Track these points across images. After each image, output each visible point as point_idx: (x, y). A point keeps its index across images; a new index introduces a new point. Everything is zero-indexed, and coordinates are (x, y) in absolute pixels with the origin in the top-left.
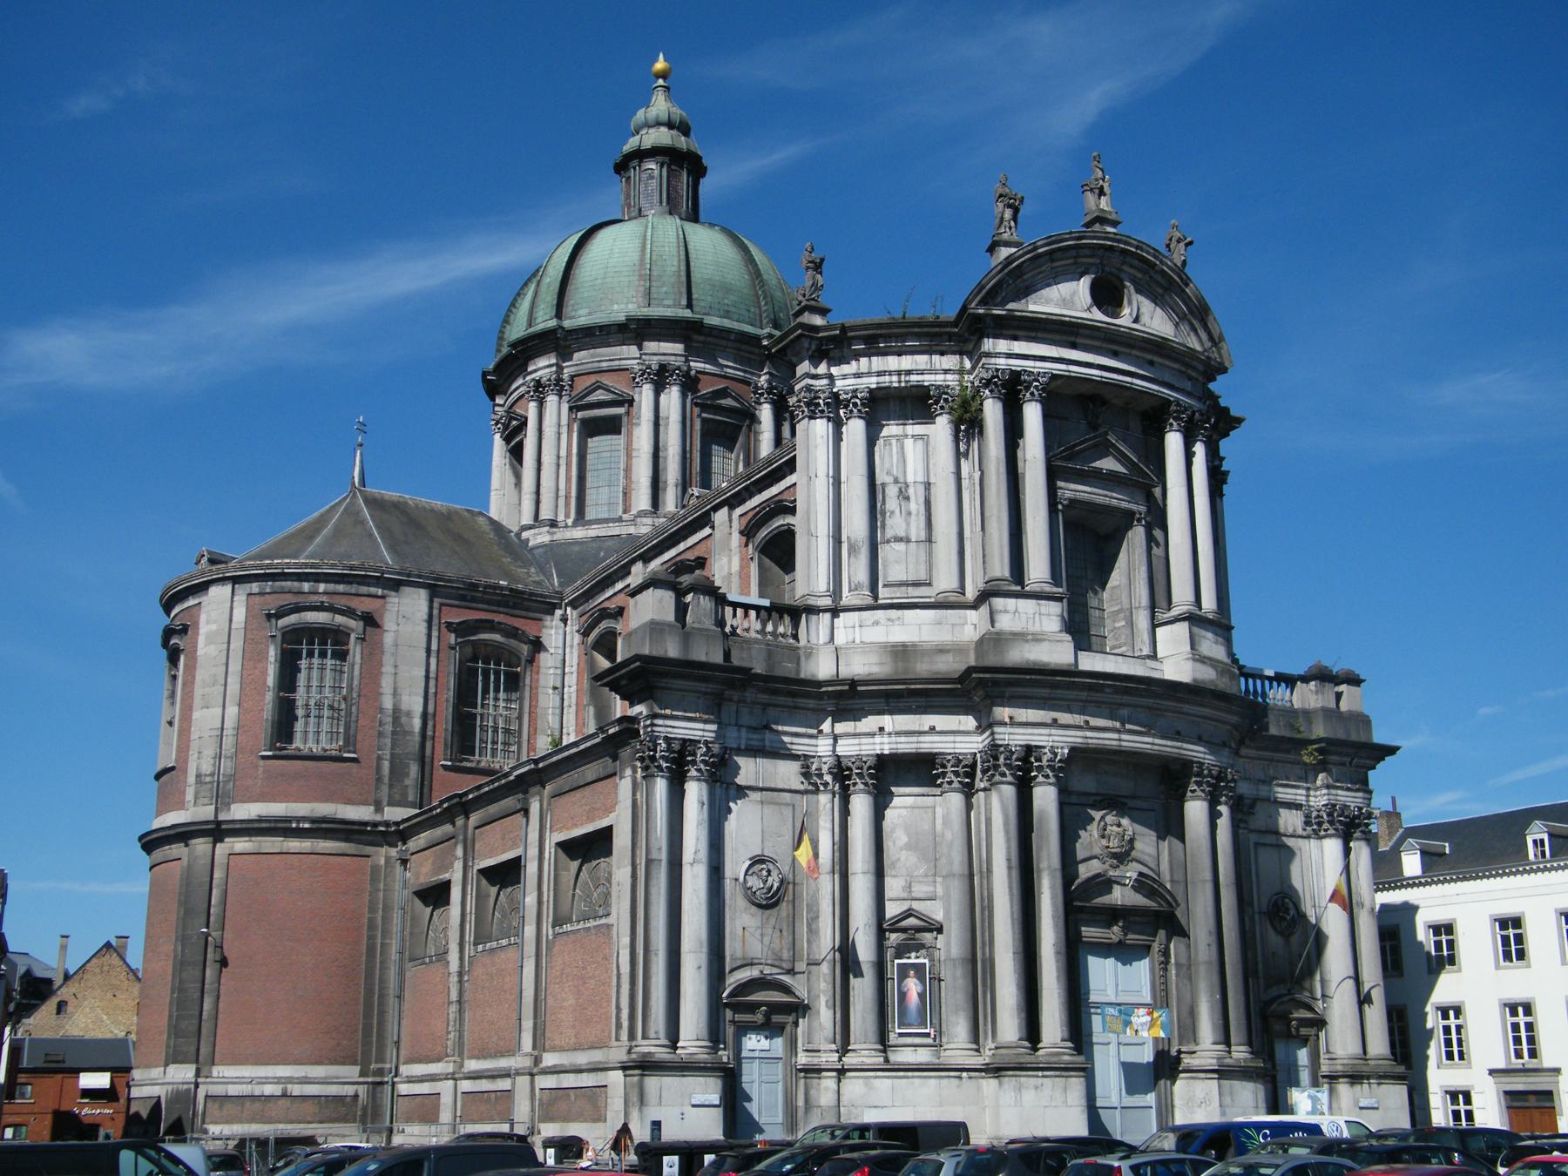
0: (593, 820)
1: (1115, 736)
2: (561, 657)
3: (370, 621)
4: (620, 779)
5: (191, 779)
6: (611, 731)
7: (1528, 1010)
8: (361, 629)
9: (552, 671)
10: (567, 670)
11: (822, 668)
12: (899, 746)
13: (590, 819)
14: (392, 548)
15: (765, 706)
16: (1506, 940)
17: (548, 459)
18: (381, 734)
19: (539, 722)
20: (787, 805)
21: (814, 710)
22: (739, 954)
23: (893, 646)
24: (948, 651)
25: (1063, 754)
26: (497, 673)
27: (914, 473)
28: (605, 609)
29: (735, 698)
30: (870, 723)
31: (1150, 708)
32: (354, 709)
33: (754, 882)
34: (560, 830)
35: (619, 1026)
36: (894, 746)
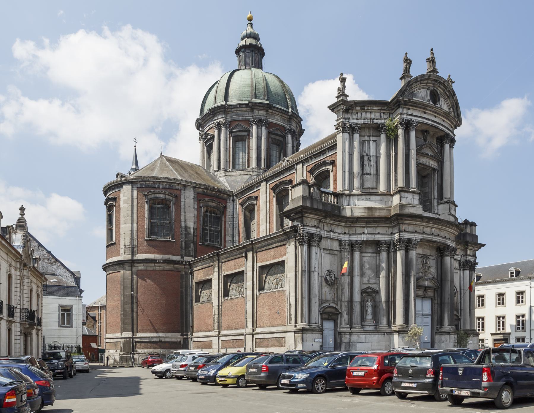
0: (276, 258)
1: (431, 237)
2: (232, 212)
3: (177, 198)
4: (289, 245)
5: (122, 246)
6: (286, 231)
8: (174, 200)
9: (230, 217)
10: (235, 216)
12: (369, 238)
13: (274, 258)
14: (181, 176)
15: (331, 224)
18: (181, 234)
19: (227, 232)
20: (336, 255)
21: (344, 226)
22: (324, 299)
23: (368, 207)
24: (384, 209)
25: (418, 242)
26: (214, 216)
28: (250, 197)
29: (324, 221)
30: (359, 230)
31: (440, 229)
32: (173, 226)
33: (328, 278)
34: (261, 262)
35: (290, 319)
36: (367, 238)
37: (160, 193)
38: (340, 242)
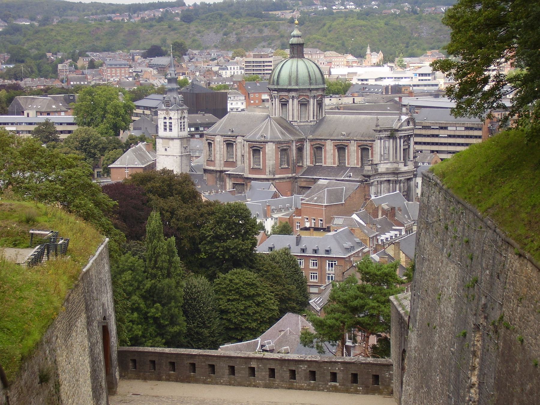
11: (380, 171)
17: (295, 110)
27: (387, 146)
30: (383, 176)
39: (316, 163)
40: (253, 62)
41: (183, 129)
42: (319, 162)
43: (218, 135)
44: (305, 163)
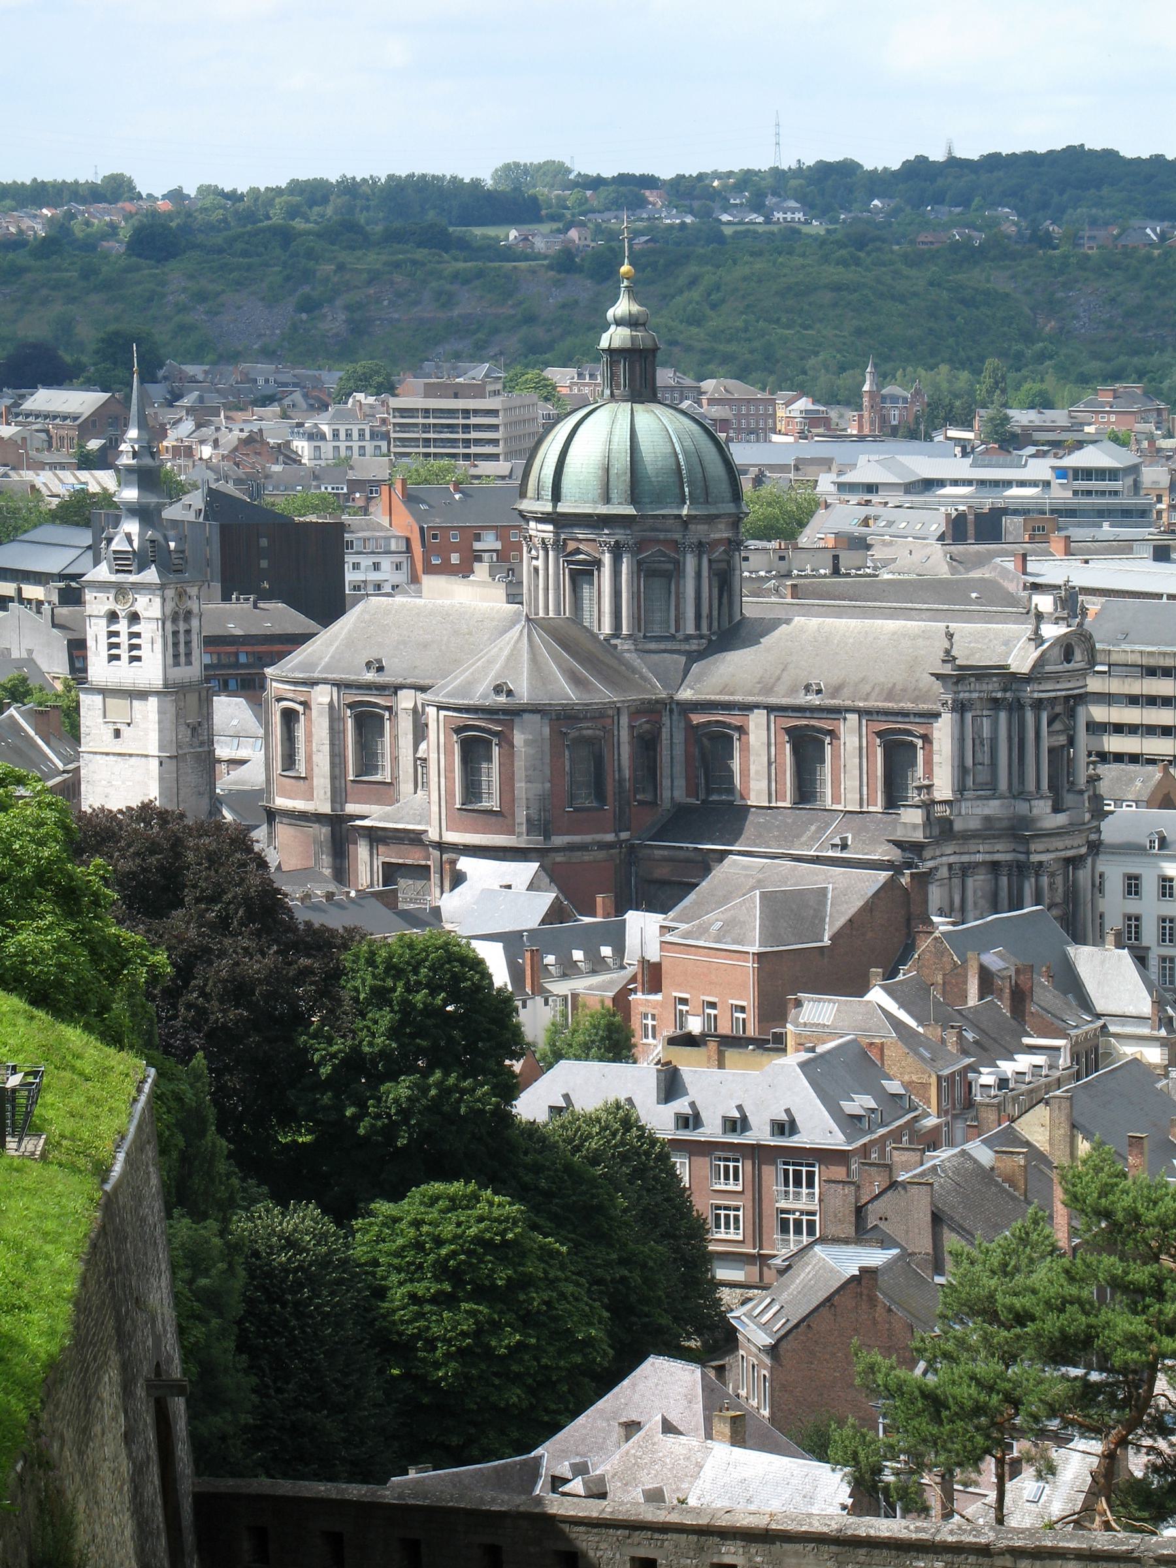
7: (1137, 919)
16: (1130, 885)
30: (973, 848)
37: (588, 728)
38: (950, 866)
39: (709, 791)
40: (427, 411)
41: (182, 659)
42: (719, 791)
43: (325, 681)
44: (666, 794)
